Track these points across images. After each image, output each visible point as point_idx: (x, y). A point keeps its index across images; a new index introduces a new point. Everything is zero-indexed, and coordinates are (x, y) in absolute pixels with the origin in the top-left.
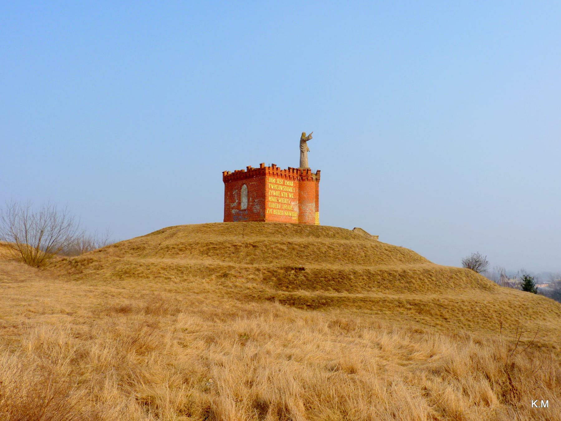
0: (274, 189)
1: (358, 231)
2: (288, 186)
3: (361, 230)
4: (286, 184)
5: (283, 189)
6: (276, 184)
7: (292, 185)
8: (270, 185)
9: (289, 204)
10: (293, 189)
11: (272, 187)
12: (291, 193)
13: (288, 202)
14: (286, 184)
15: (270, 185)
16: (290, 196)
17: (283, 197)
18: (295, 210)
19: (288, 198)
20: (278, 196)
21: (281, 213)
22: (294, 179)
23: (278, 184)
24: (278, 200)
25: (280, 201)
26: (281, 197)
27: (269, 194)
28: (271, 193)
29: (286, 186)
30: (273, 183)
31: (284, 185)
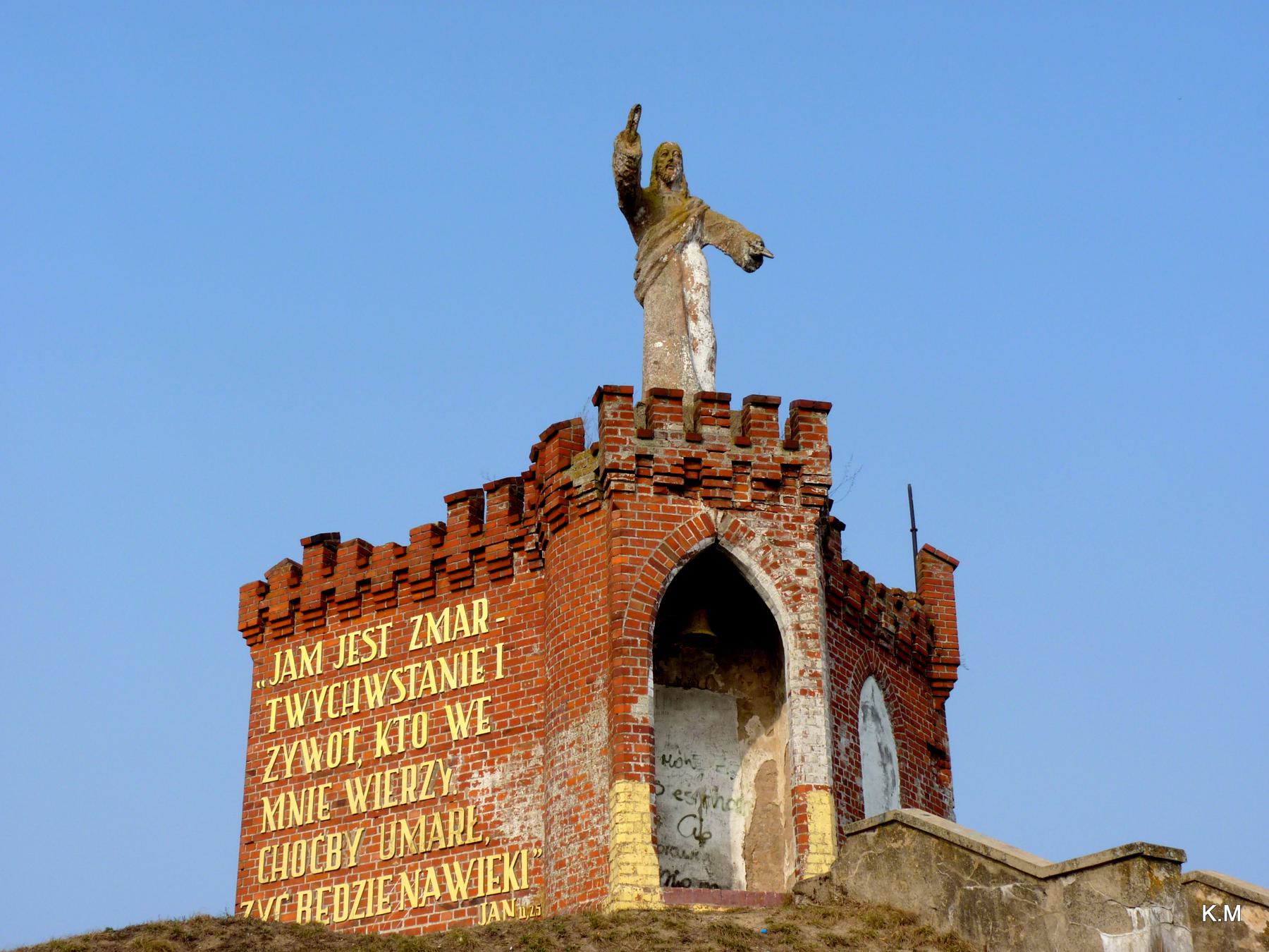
0: (311, 727)
1: (871, 866)
2: (442, 648)
3: (909, 839)
4: (422, 637)
5: (392, 691)
6: (328, 675)
7: (480, 625)
8: (281, 708)
9: (449, 799)
10: (487, 661)
11: (296, 717)
12: (461, 694)
13: (437, 783)
14: (422, 637)
15: (281, 708)
16: (459, 726)
17: (393, 759)
18: (511, 829)
19: (441, 746)
20: (344, 770)
21: (363, 903)
22: (501, 570)
23: (350, 671)
24: (343, 803)
25: (357, 802)
26: (371, 765)
27: (266, 779)
28: (279, 766)
29: (421, 654)
30: (306, 683)
31: (398, 655)
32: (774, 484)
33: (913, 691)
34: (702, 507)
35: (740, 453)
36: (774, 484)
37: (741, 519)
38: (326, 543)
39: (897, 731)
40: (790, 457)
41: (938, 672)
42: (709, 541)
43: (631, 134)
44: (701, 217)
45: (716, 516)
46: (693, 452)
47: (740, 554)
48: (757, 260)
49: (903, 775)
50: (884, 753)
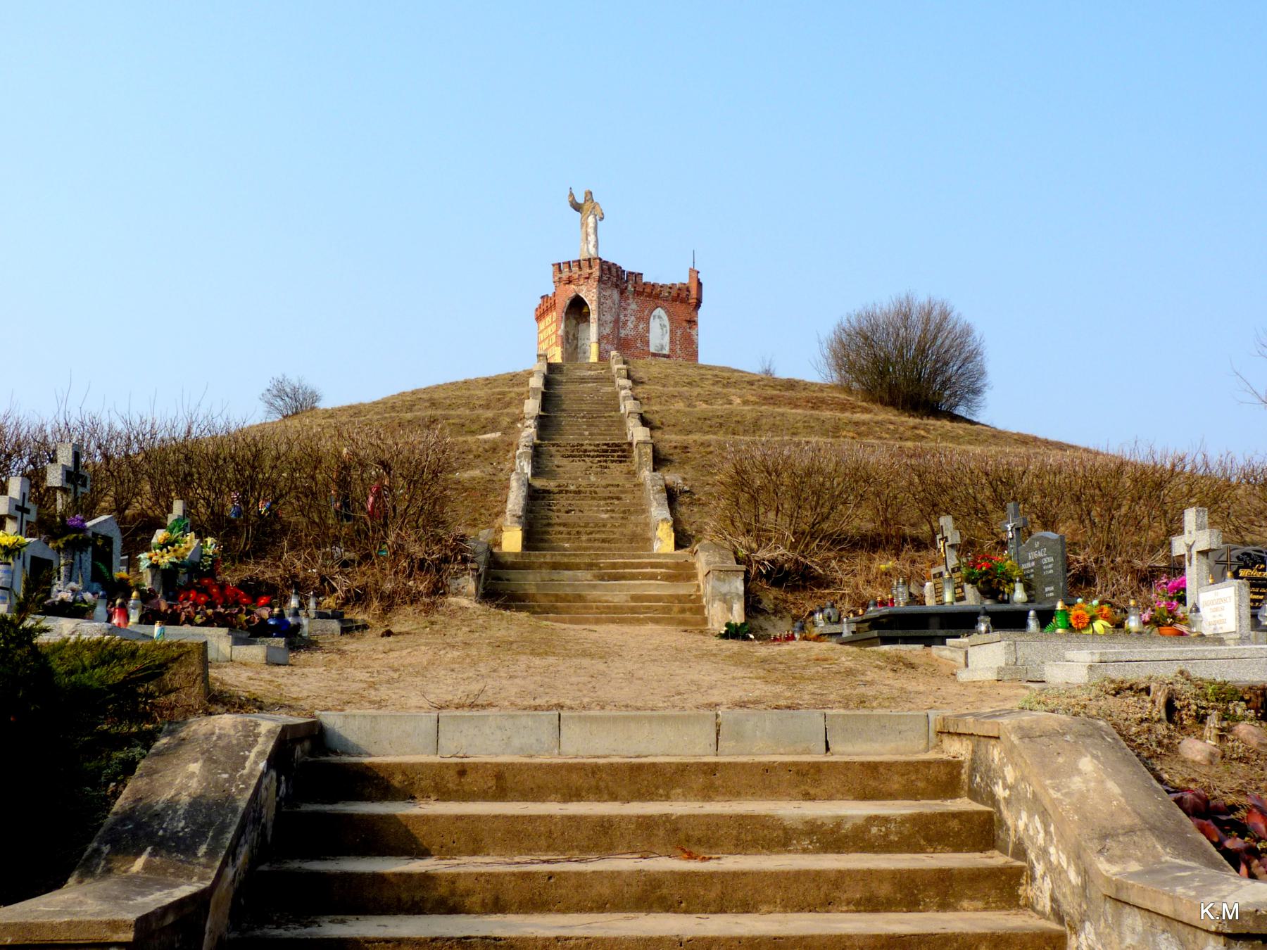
32: (588, 278)
33: (681, 309)
34: (573, 286)
35: (580, 273)
36: (588, 278)
37: (581, 287)
38: (543, 297)
39: (669, 320)
40: (590, 271)
41: (691, 301)
42: (574, 294)
43: (571, 194)
44: (594, 208)
45: (575, 287)
46: (571, 274)
47: (581, 295)
48: (602, 219)
49: (671, 331)
50: (662, 326)
